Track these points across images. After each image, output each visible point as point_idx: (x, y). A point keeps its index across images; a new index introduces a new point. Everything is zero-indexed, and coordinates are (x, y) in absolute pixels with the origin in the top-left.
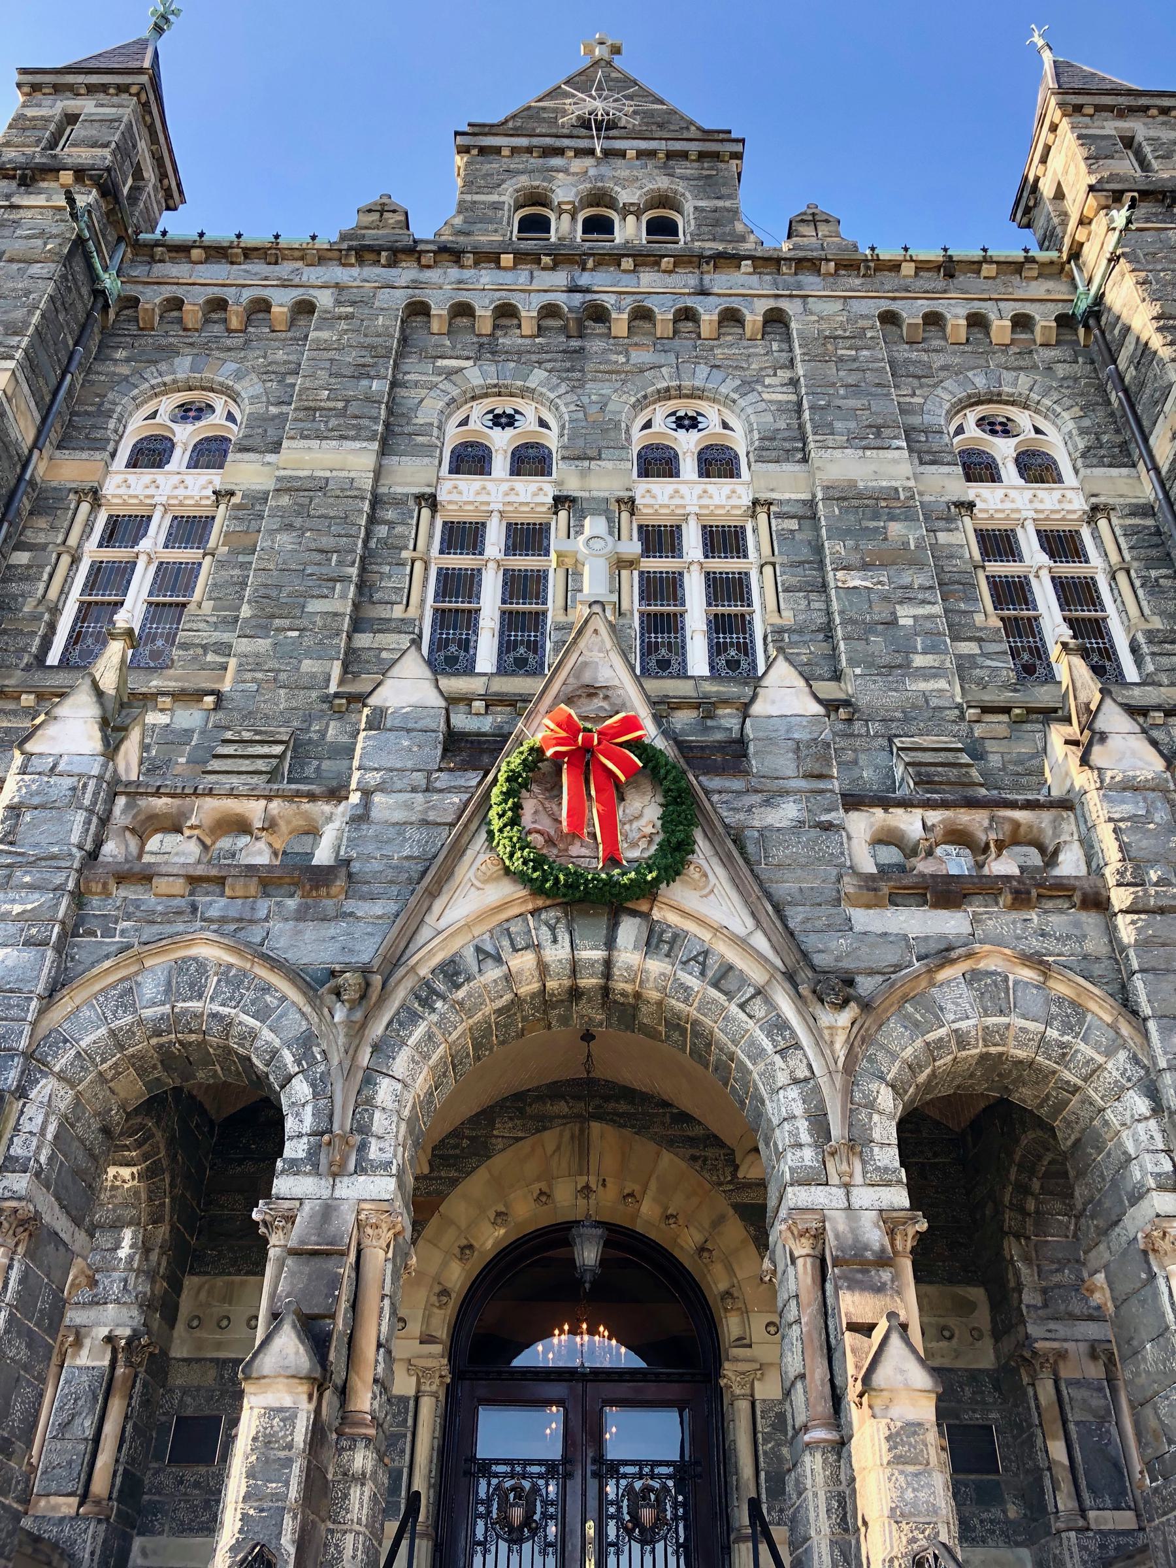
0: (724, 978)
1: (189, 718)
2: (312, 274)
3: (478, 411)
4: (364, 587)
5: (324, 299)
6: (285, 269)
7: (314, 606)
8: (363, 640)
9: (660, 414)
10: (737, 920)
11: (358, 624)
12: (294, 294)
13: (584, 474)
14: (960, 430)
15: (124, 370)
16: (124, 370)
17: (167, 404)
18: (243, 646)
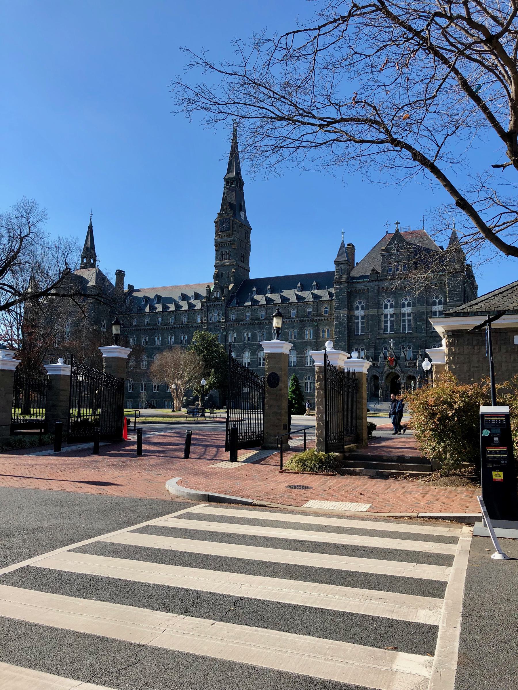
0: (398, 372)
1: (367, 341)
2: (368, 284)
3: (386, 300)
4: (378, 326)
5: (370, 288)
6: (365, 284)
7: (375, 329)
8: (379, 331)
9: (404, 299)
10: (399, 369)
11: (378, 330)
12: (367, 288)
13: (396, 310)
14: (433, 299)
15: (353, 299)
16: (353, 299)
17: (357, 302)
18: (370, 333)
